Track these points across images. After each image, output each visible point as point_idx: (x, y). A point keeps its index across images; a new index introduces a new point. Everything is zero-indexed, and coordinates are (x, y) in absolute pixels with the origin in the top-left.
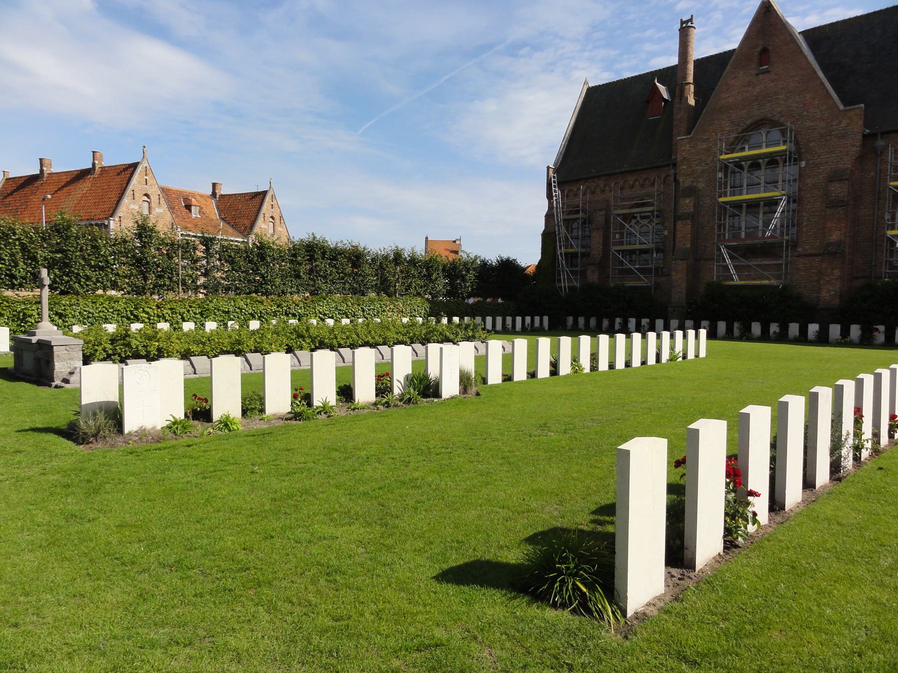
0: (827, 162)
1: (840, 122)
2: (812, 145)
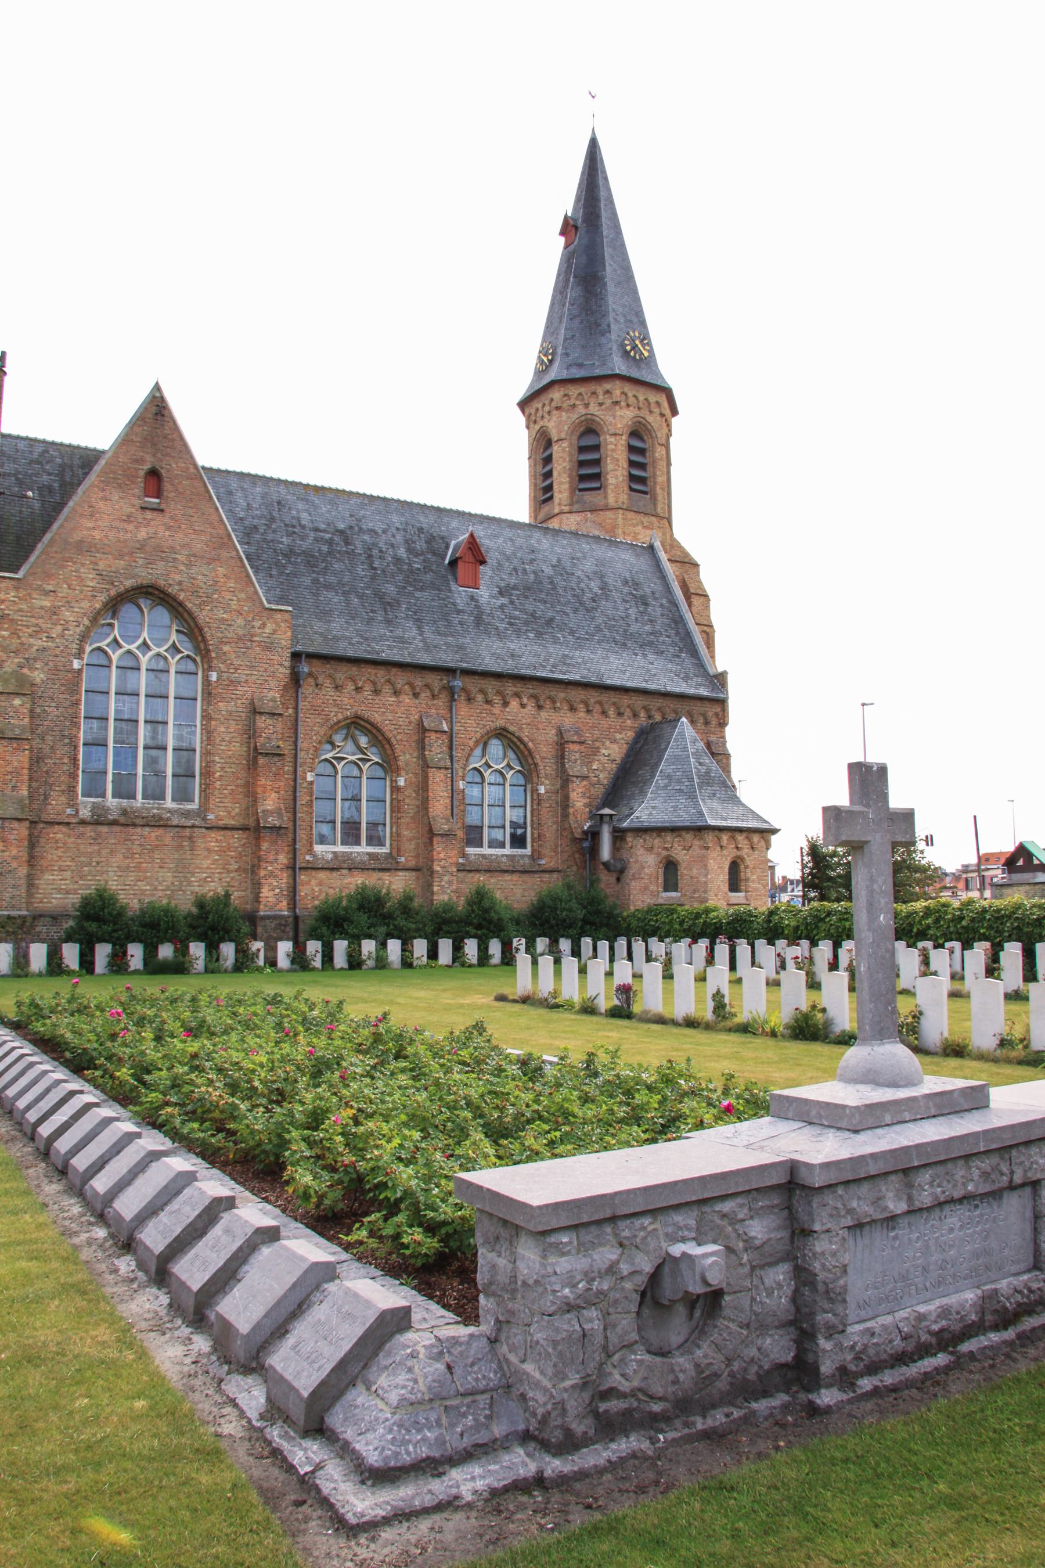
0: (246, 681)
1: (264, 625)
2: (226, 648)
